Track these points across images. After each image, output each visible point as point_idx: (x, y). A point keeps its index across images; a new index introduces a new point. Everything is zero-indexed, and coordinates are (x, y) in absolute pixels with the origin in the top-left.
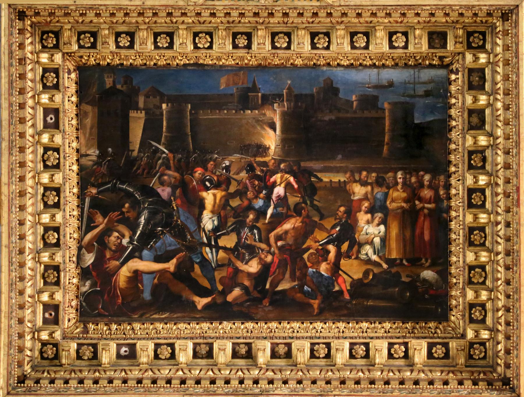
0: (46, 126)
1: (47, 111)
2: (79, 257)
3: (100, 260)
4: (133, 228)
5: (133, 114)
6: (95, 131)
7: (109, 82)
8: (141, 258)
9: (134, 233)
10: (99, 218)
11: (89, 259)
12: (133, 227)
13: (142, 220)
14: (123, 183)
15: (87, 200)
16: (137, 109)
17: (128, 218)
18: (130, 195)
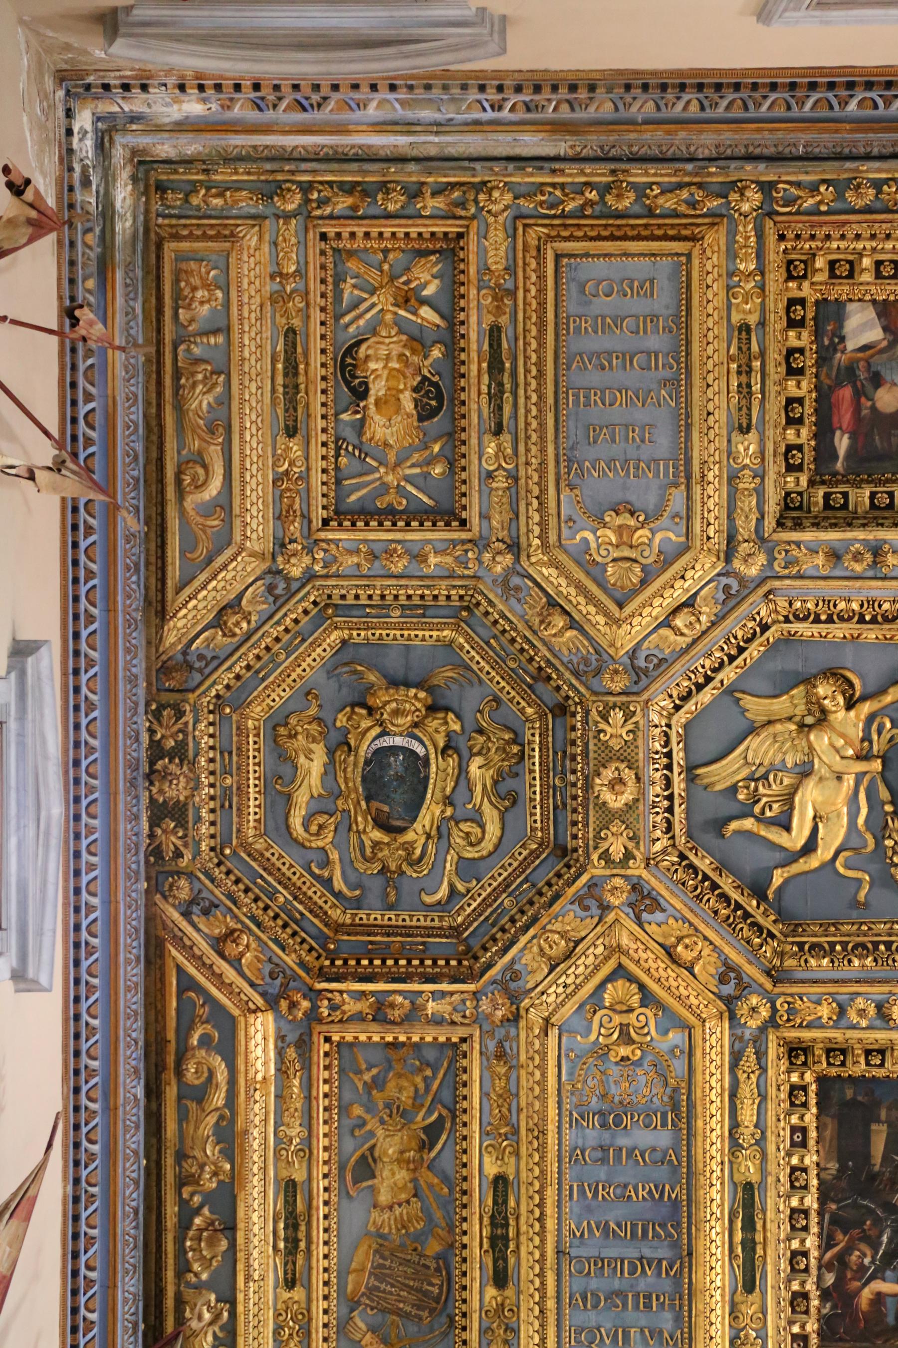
0: (793, 1144)
1: (794, 1129)
2: (820, 1277)
3: (840, 1280)
4: (875, 1247)
5: (874, 1127)
6: (835, 1142)
7: (849, 1093)
8: (884, 1280)
9: (877, 1253)
10: (840, 1236)
11: (830, 1279)
12: (875, 1245)
13: (885, 1238)
14: (864, 1199)
15: (827, 1217)
16: (878, 1121)
17: (869, 1237)
18: (871, 1212)
